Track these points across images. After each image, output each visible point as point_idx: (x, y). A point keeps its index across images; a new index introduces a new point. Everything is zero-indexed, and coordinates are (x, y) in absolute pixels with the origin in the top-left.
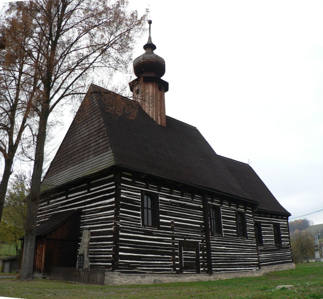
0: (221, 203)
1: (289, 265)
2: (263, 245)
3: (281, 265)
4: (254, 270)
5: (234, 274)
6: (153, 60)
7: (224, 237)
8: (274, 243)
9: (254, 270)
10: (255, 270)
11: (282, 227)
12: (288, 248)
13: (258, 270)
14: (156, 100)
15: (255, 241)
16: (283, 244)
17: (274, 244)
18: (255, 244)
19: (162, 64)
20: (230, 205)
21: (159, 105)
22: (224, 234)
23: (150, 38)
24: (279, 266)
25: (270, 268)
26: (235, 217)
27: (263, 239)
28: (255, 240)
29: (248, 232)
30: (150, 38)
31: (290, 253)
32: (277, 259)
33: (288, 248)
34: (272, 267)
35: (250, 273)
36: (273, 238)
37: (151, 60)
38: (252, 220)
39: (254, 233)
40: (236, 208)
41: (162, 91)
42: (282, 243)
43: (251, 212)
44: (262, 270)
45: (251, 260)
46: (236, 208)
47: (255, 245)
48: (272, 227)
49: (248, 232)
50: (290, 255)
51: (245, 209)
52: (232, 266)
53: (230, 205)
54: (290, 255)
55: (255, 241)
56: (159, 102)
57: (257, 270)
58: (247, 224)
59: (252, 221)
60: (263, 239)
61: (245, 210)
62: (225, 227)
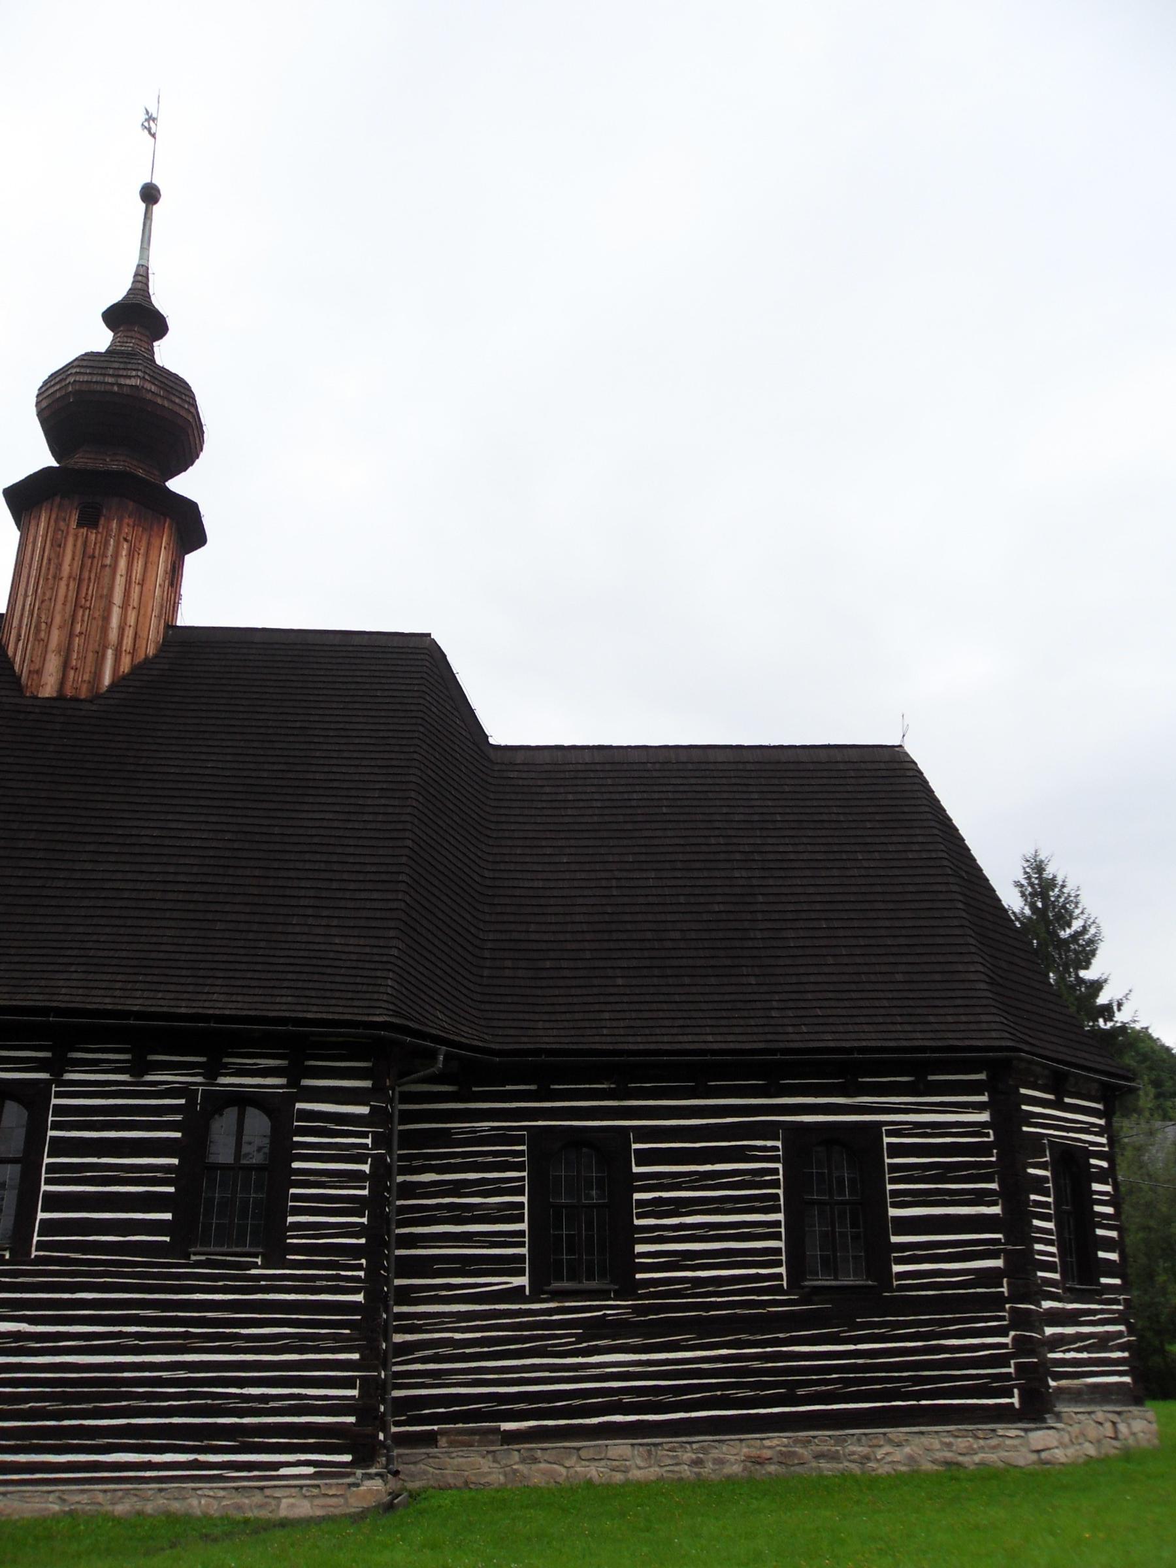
0: (57, 1066)
1: (961, 1443)
2: (629, 1288)
3: (840, 1441)
4: (283, 1471)
5: (51, 1497)
6: (63, 393)
7: (39, 1260)
8: (782, 1270)
9: (283, 1471)
10: (310, 1470)
11: (896, 1150)
12: (997, 1301)
13: (348, 1475)
14: (51, 581)
15: (362, 1274)
16: (902, 1275)
17: (779, 1276)
18: (355, 1291)
19: (116, 388)
20: (139, 1067)
21: (64, 604)
22: (41, 1246)
23: (142, 277)
24: (806, 1442)
25: (688, 1456)
26: (179, 1135)
27: (639, 1248)
28: (359, 1267)
29: (290, 1219)
30: (142, 277)
31: (1004, 1346)
32: (801, 1392)
33: (997, 1301)
34: (704, 1451)
35: (222, 1493)
36: (777, 1236)
37: (58, 395)
38: (364, 1135)
39: (365, 1220)
40: (199, 1079)
41: (102, 521)
42: (897, 1268)
43: (367, 1084)
44: (370, 1477)
45: (272, 1404)
46: (199, 1079)
47: (359, 1298)
48: (775, 1159)
49: (290, 1219)
50: (1002, 1361)
51: (294, 1074)
52: (61, 1440)
53: (139, 1067)
54: (1002, 1361)
55: (362, 1274)
56: (68, 585)
57: (325, 1472)
58: (296, 1165)
59: (365, 1146)
60: (639, 1248)
61: (293, 1082)
62: (54, 1202)
